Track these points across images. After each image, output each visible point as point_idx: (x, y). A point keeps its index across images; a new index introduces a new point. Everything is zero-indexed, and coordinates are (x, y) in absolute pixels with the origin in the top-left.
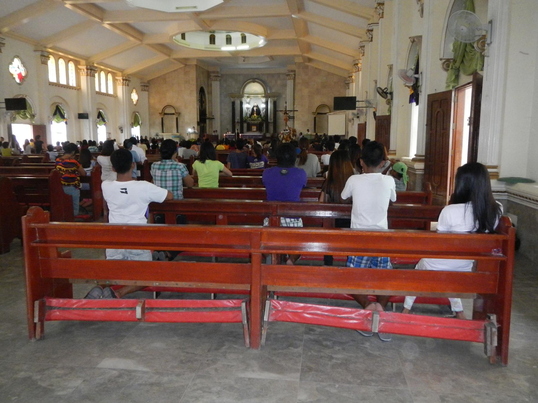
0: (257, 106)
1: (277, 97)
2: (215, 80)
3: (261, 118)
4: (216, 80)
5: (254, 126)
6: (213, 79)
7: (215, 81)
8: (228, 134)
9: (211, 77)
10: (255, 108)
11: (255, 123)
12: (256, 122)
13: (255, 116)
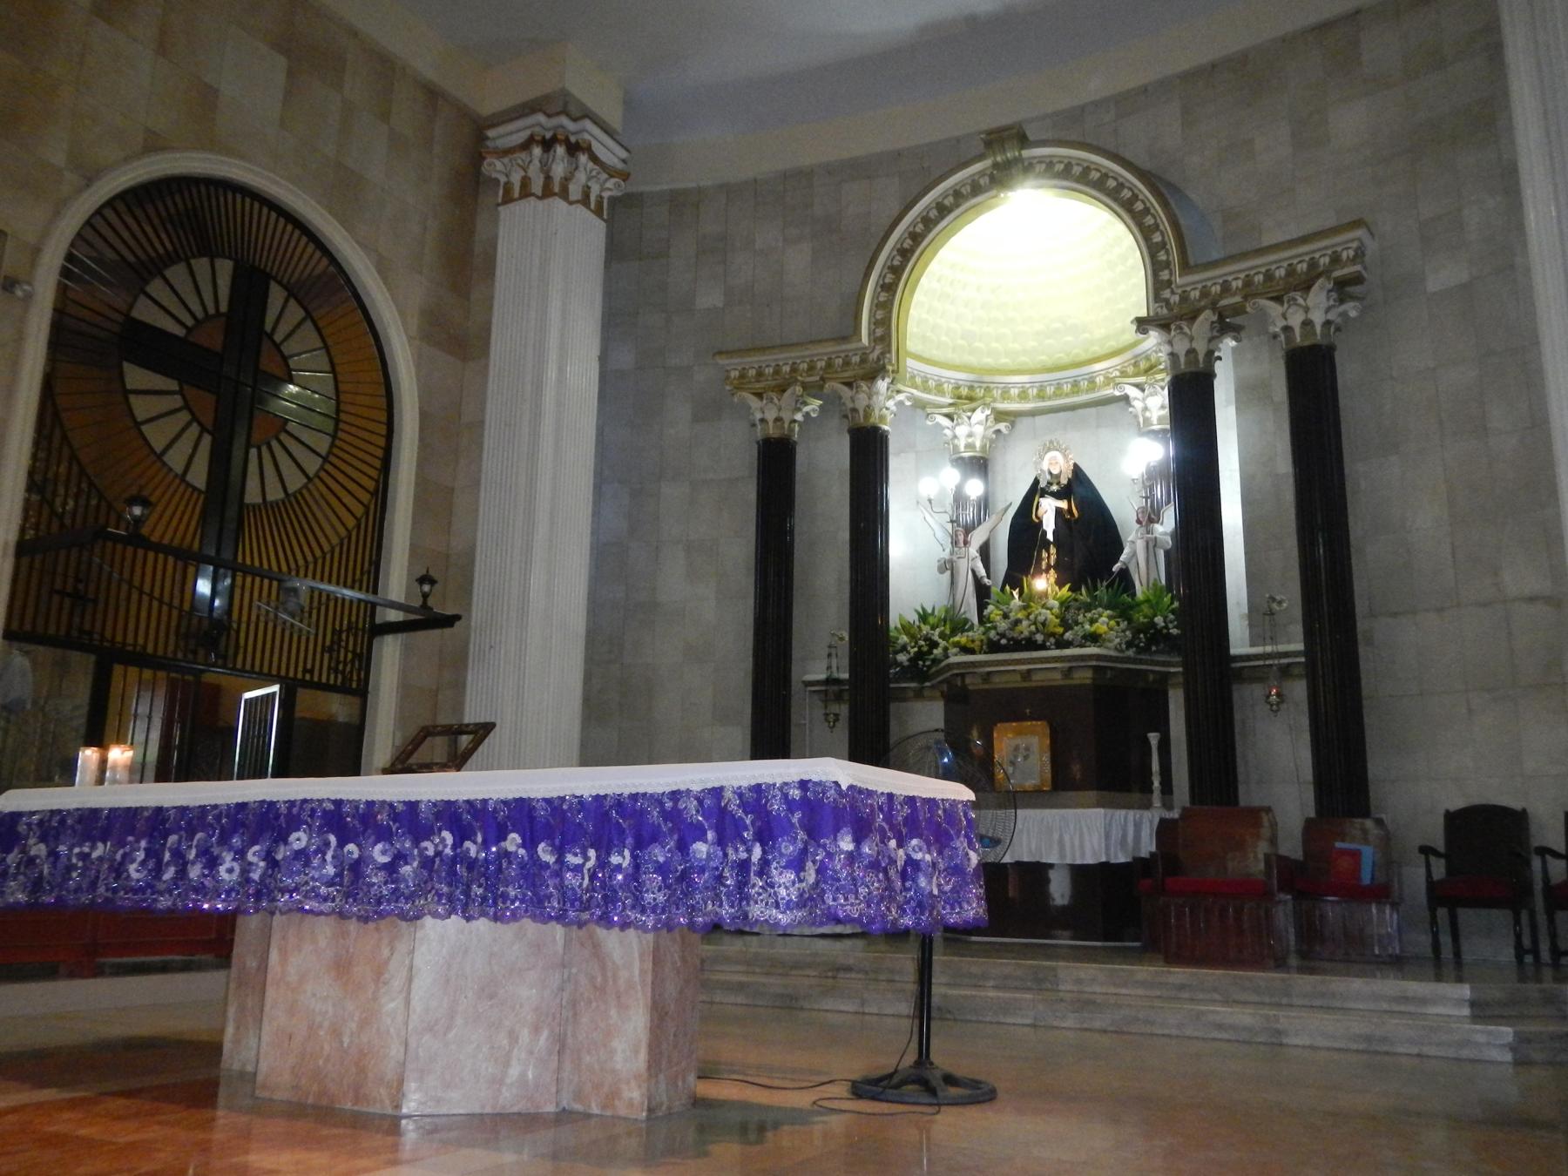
0: (1077, 487)
1: (1343, 288)
2: (537, 187)
3: (1124, 612)
4: (547, 192)
5: (1020, 718)
6: (516, 178)
7: (526, 192)
8: (79, 795)
9: (495, 167)
10: (1048, 510)
11: (1038, 679)
12: (1047, 665)
13: (1029, 599)
